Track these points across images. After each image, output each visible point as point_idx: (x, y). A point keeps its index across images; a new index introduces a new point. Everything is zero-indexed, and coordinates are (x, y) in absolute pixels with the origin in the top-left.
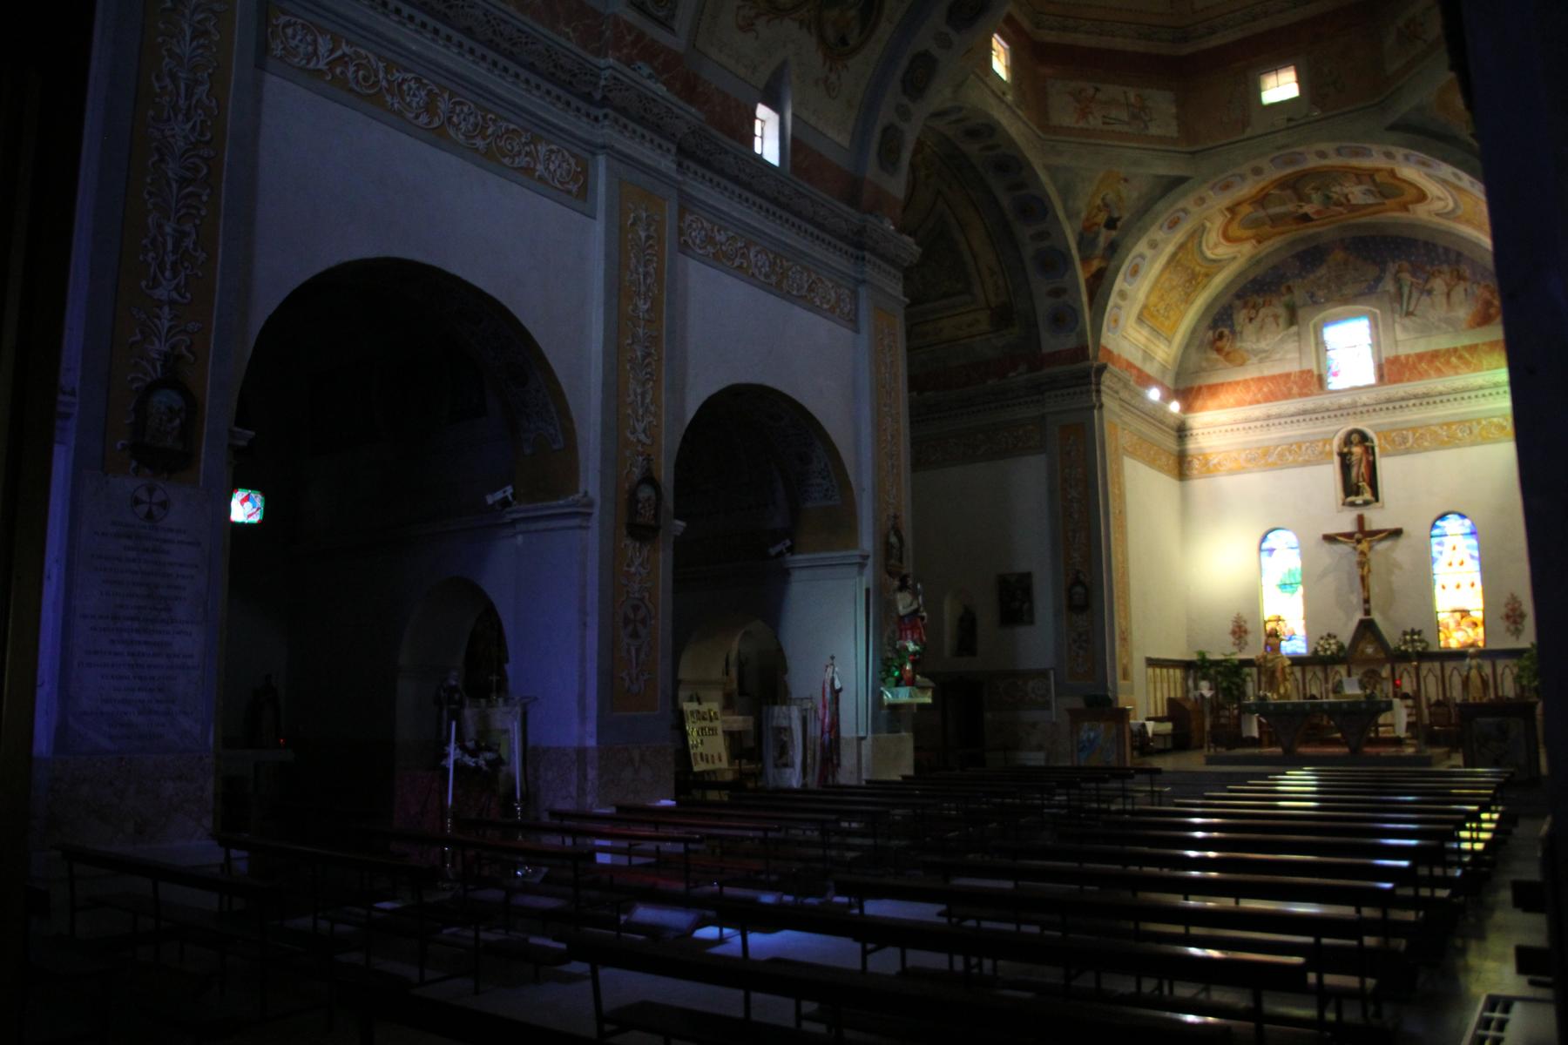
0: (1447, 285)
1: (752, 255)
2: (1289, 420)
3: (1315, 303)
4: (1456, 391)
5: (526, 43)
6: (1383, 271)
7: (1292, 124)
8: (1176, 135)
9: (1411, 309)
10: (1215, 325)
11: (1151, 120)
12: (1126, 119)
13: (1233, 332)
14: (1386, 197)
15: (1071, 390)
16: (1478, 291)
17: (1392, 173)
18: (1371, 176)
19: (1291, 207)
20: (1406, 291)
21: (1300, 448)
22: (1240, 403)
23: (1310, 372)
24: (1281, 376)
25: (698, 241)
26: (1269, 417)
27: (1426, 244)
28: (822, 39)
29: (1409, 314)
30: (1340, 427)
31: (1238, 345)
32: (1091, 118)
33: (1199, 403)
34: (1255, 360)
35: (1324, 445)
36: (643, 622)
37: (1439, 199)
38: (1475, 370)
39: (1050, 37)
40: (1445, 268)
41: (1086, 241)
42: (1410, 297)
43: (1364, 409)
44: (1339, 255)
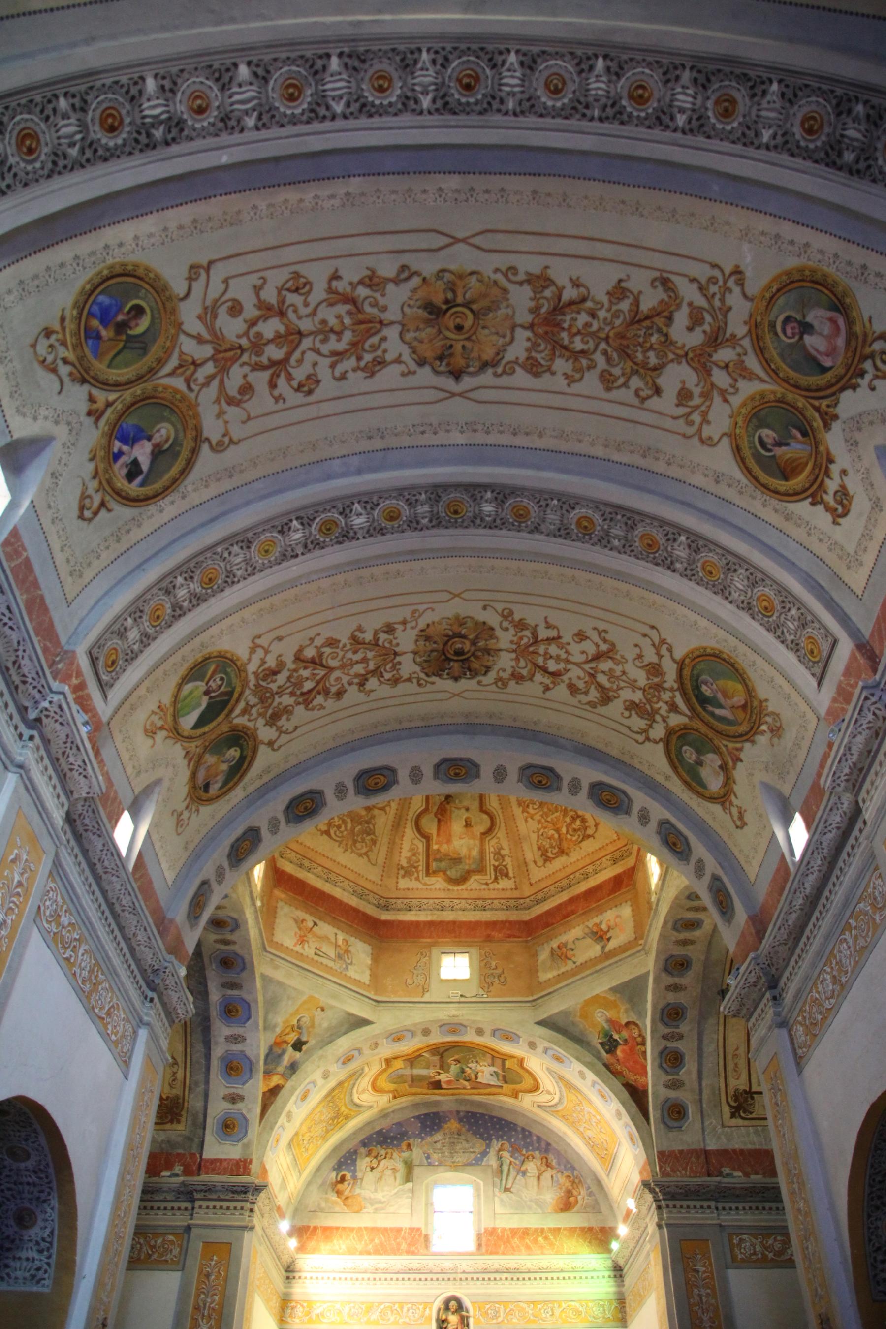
0: (538, 1169)
1: (81, 951)
2: (395, 1276)
3: (430, 1164)
4: (541, 1270)
5: (5, 624)
6: (488, 1146)
7: (463, 999)
8: (367, 983)
9: (509, 1186)
10: (338, 1167)
11: (351, 964)
12: (333, 956)
13: (354, 1178)
14: (506, 1082)
15: (225, 1204)
16: (562, 1180)
17: (521, 1062)
18: (504, 1061)
19: (431, 1072)
20: (505, 1168)
21: (402, 1308)
22: (351, 1251)
23: (419, 1229)
24: (392, 1229)
25: (48, 913)
26: (376, 1271)
27: (523, 1130)
28: (194, 775)
29: (507, 1190)
30: (439, 1291)
31: (358, 1191)
32: (306, 945)
33: (312, 1244)
34: (370, 1209)
35: (425, 1309)
37: (549, 1093)
38: (557, 1253)
39: (289, 868)
40: (537, 1154)
41: (273, 1056)
42: (508, 1175)
43: (463, 1276)
44: (453, 1125)
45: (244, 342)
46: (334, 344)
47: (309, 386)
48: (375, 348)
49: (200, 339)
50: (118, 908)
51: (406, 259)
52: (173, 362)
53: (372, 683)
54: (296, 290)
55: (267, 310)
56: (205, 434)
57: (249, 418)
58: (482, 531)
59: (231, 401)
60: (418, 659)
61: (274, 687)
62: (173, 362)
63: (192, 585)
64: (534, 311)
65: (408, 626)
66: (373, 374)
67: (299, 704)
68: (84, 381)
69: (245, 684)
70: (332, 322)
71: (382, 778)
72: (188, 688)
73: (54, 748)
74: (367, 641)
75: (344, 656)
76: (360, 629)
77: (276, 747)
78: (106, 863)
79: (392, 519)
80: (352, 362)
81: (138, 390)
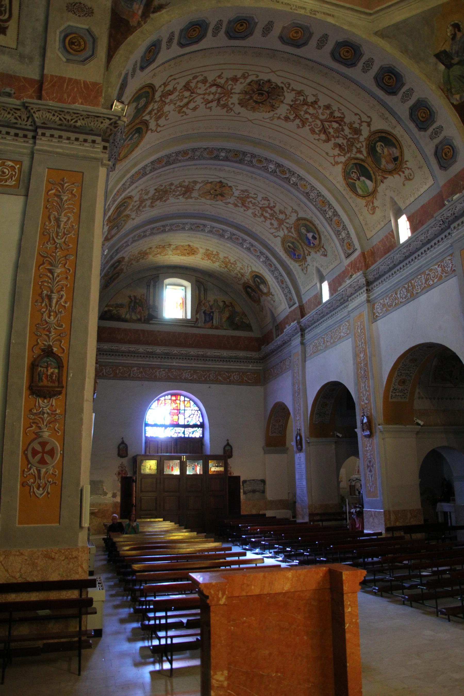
28: (390, 172)
36: (372, 466)
45: (274, 219)
46: (253, 201)
47: (266, 199)
48: (243, 194)
49: (283, 229)
50: (407, 254)
51: (226, 206)
52: (290, 234)
53: (311, 99)
54: (256, 214)
55: (265, 217)
56: (296, 218)
57: (285, 208)
58: (228, 148)
59: (286, 215)
60: (282, 98)
61: (345, 142)
62: (290, 234)
63: (327, 210)
64: (191, 193)
65: (278, 116)
66: (246, 190)
67: (345, 123)
68: (306, 258)
69: (350, 159)
70: (251, 205)
71: (342, 53)
72: (360, 192)
73: (353, 292)
74: (299, 120)
75: (313, 121)
76: (298, 127)
77: (369, 120)
78: (389, 263)
79: (260, 161)
80: (250, 195)
81: (300, 241)
